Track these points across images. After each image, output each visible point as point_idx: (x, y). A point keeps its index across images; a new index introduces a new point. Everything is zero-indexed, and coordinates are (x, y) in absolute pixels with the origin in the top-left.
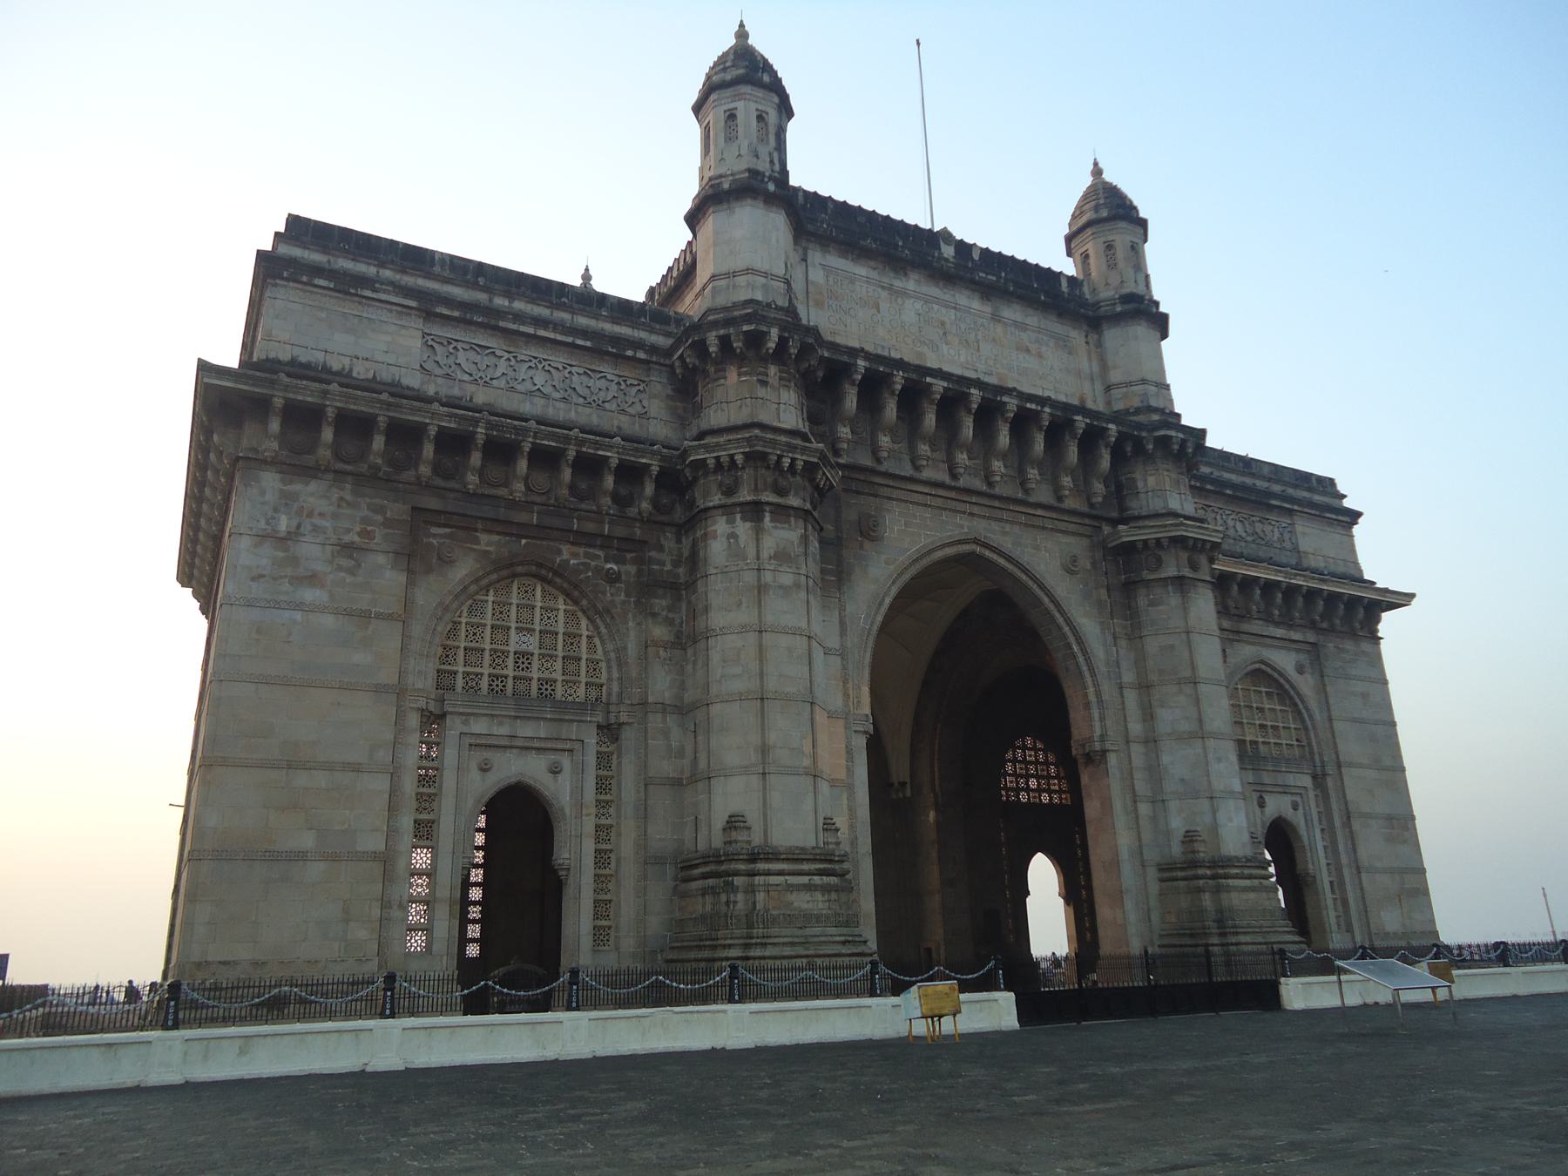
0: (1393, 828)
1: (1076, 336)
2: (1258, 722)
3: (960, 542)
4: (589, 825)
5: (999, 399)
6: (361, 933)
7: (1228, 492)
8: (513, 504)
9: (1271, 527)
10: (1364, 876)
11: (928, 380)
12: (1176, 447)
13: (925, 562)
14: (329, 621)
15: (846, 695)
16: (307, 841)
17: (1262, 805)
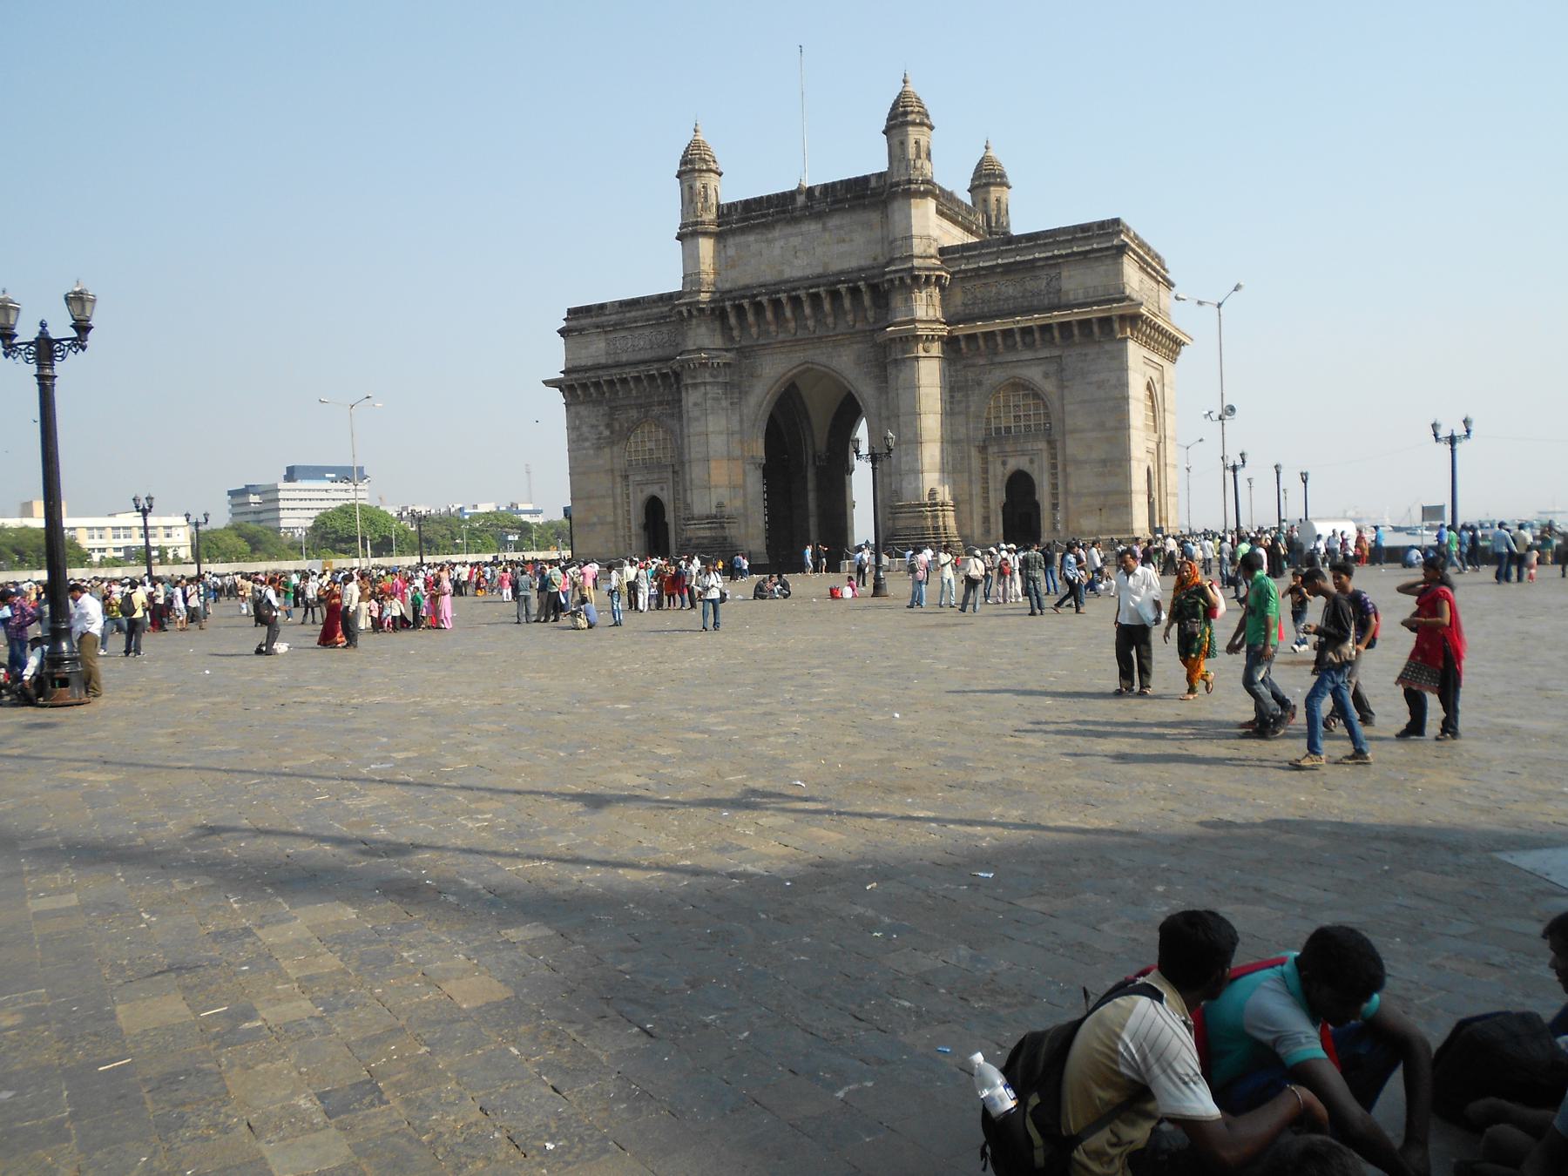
0: (1106, 466)
1: (875, 217)
2: (1012, 415)
3: (798, 366)
4: (672, 508)
5: (794, 293)
6: (611, 545)
7: (998, 270)
8: (637, 398)
9: (1040, 281)
10: (1070, 500)
11: (759, 299)
12: (897, 282)
13: (784, 378)
14: (591, 452)
15: (742, 449)
16: (595, 519)
17: (1004, 463)
